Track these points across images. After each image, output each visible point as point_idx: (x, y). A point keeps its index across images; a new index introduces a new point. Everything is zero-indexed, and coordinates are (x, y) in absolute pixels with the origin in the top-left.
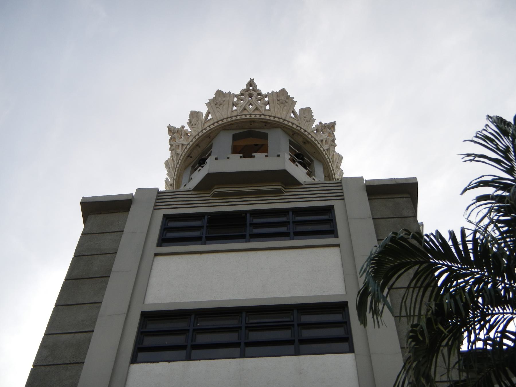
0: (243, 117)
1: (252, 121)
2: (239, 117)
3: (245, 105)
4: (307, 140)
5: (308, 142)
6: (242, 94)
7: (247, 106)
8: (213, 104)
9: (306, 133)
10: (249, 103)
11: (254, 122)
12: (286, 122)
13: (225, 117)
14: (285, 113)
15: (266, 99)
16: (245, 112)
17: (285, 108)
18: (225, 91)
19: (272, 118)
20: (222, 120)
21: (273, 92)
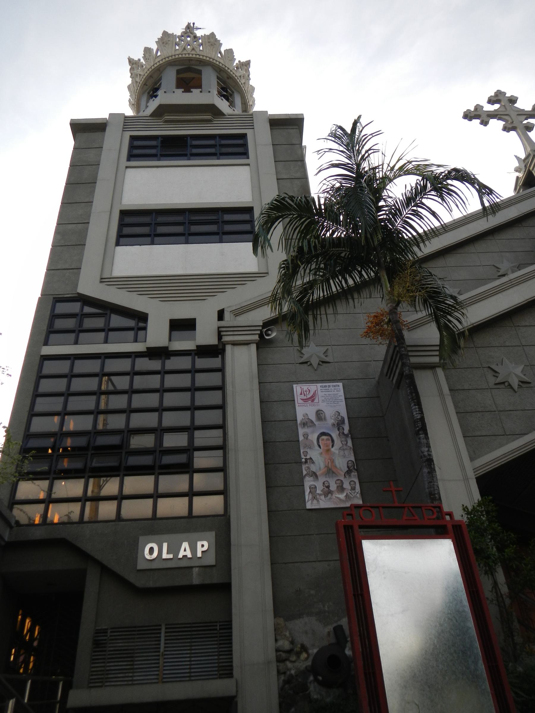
0: (184, 56)
1: (190, 60)
2: (180, 56)
3: (185, 46)
4: (230, 76)
5: (231, 77)
6: (182, 36)
8: (161, 43)
9: (229, 71)
10: (188, 44)
11: (191, 60)
12: (215, 61)
13: (170, 55)
14: (214, 53)
16: (185, 52)
17: (214, 49)
18: (170, 32)
19: (204, 58)
20: (168, 57)
21: (205, 35)
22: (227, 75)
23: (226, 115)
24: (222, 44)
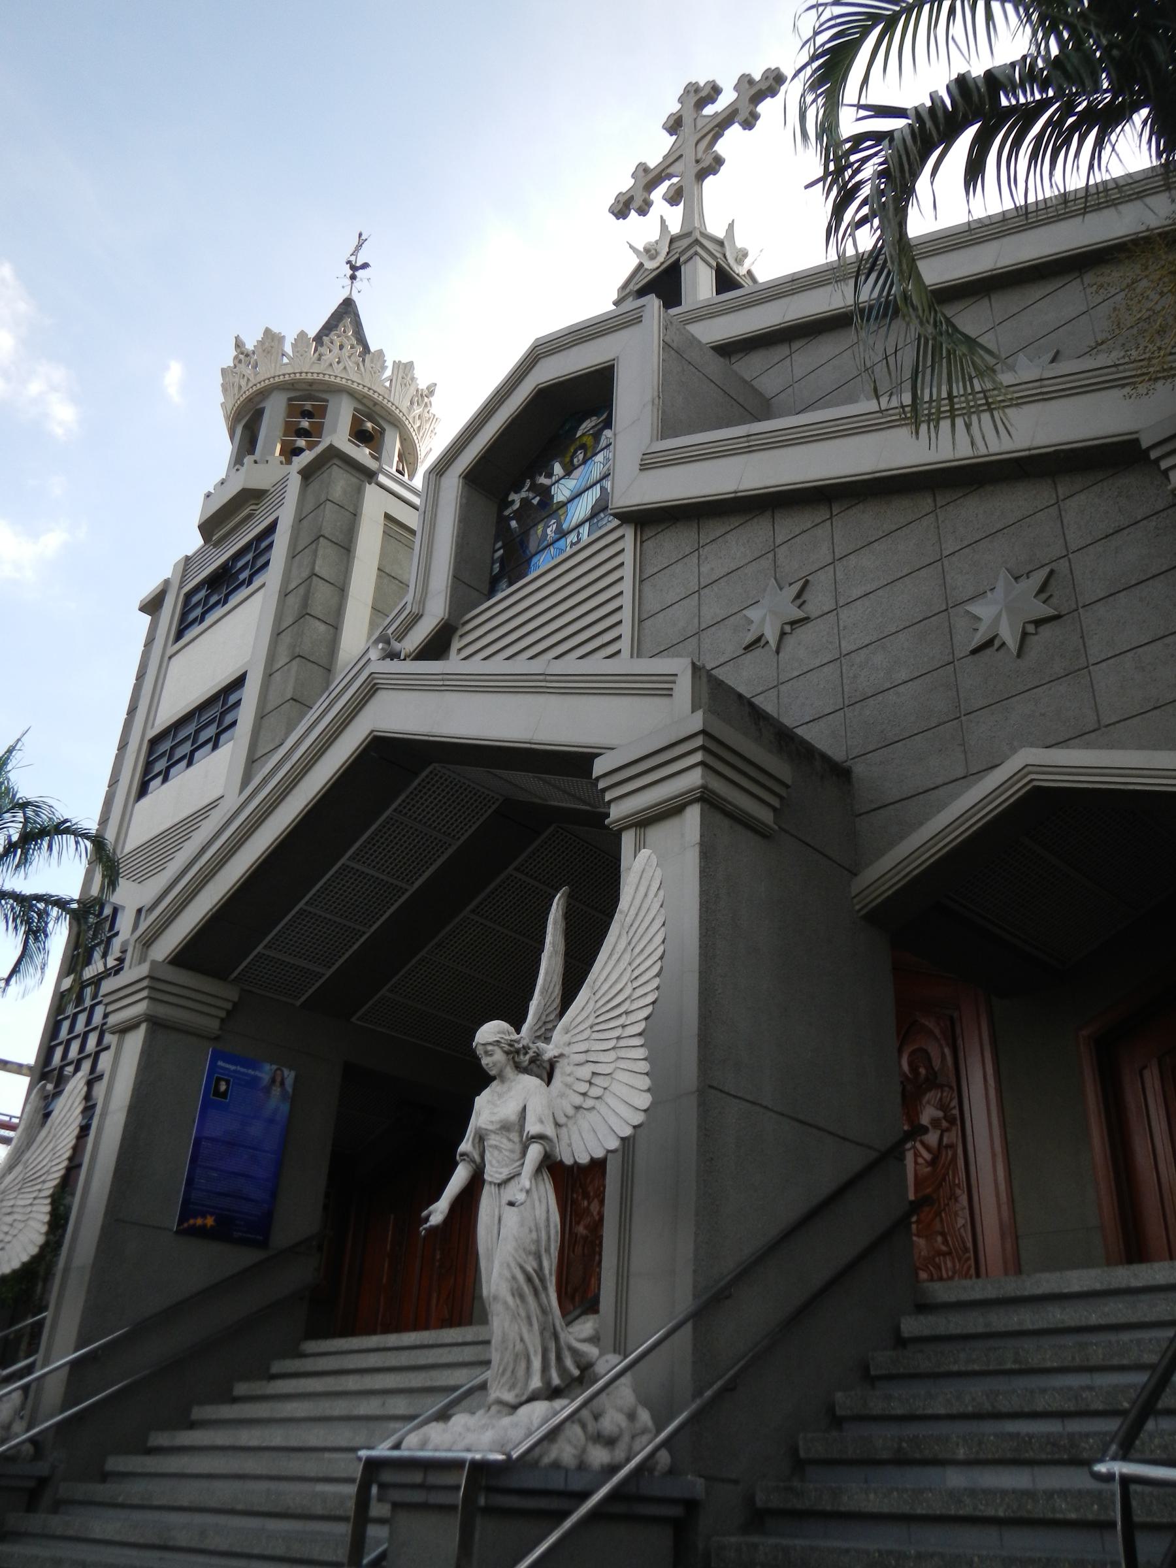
0: (241, 399)
1: (250, 400)
6: (235, 366)
7: (241, 380)
14: (273, 365)
15: (255, 357)
21: (258, 341)
22: (304, 383)
23: (269, 490)
24: (284, 337)
